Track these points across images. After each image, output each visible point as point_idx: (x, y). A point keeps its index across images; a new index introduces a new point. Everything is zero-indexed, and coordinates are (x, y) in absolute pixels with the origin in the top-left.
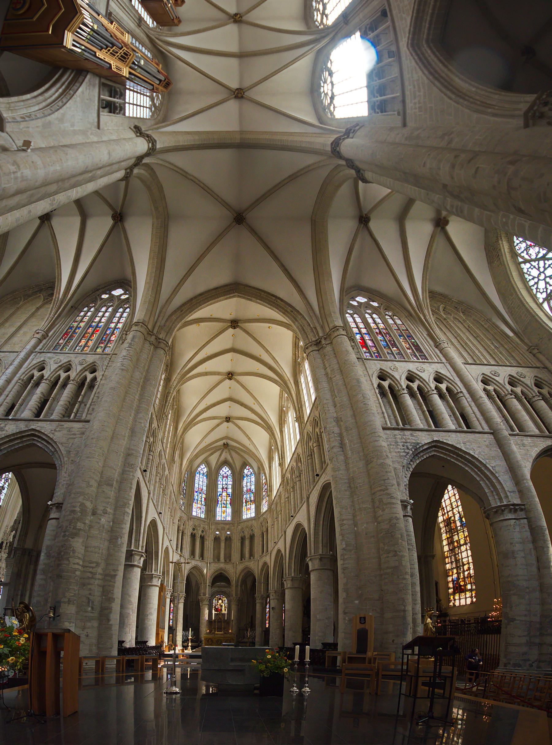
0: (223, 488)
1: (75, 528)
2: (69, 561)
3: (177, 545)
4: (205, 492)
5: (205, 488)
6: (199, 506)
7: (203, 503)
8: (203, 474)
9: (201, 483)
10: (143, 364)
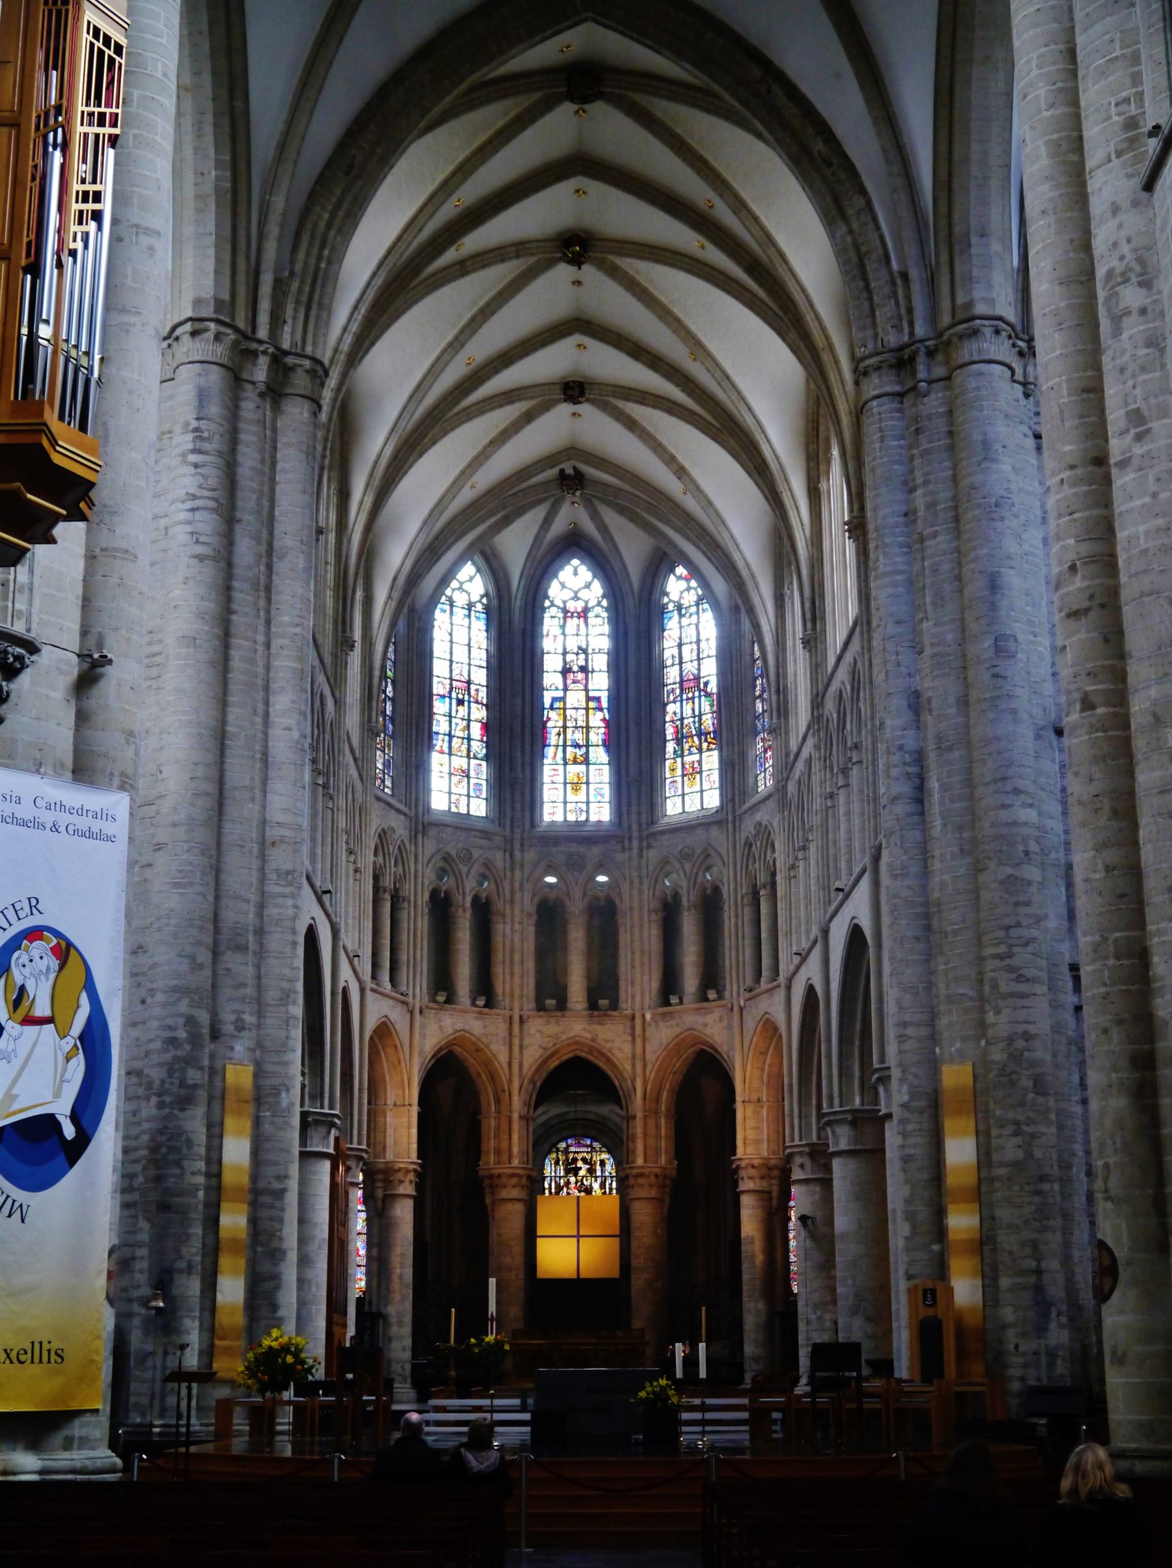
0: (566, 671)
1: (182, 1084)
2: (182, 1168)
3: (375, 954)
4: (483, 695)
5: (480, 677)
6: (460, 762)
7: (478, 748)
8: (470, 606)
9: (460, 654)
10: (254, 496)
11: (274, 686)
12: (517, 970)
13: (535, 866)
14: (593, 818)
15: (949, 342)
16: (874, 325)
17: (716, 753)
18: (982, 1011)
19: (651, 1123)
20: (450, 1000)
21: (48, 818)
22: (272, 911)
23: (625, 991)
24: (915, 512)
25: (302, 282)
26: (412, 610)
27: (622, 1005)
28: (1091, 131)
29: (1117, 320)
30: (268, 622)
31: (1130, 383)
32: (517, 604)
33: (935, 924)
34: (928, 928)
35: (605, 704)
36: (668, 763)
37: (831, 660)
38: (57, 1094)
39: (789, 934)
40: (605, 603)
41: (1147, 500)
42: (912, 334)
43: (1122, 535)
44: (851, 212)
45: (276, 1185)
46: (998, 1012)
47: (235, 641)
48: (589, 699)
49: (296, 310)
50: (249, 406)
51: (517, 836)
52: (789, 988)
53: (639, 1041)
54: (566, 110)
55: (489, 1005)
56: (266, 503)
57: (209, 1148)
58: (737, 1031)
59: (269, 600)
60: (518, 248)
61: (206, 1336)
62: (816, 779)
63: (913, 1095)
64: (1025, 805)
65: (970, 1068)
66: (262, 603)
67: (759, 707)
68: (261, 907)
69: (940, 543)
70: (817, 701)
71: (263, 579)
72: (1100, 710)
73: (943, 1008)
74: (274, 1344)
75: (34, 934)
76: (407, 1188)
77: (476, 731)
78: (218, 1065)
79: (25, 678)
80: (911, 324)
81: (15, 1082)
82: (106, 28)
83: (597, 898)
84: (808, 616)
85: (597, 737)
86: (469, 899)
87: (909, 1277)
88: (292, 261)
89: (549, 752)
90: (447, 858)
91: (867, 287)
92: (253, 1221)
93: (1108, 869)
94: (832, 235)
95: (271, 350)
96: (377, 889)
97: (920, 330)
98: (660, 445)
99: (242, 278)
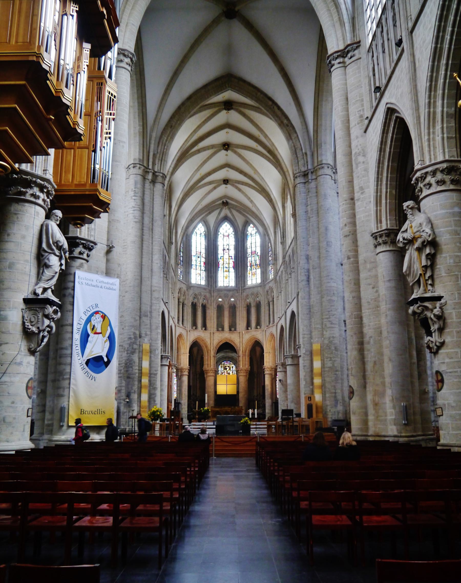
0: (224, 250)
1: (132, 348)
4: (204, 256)
5: (203, 251)
7: (203, 268)
11: (154, 253)
12: (212, 321)
13: (216, 296)
14: (230, 285)
15: (316, 170)
16: (298, 165)
17: (260, 270)
18: (323, 331)
19: (244, 358)
20: (196, 329)
21: (100, 285)
22: (154, 307)
23: (238, 326)
24: (308, 211)
25: (160, 154)
26: (187, 235)
27: (237, 330)
28: (351, 118)
29: (357, 165)
30: (152, 238)
31: (360, 180)
32: (212, 234)
33: (312, 310)
34: (310, 311)
35: (233, 258)
36: (248, 272)
37: (287, 247)
38: (103, 351)
39: (277, 313)
40: (233, 233)
41: (364, 208)
42: (308, 168)
43: (357, 217)
44: (293, 138)
45: (155, 372)
46: (326, 331)
47: (144, 242)
48: (229, 256)
49: (158, 161)
50: (148, 185)
51: (212, 289)
52: (277, 326)
53: (241, 338)
54: (224, 112)
55: (205, 330)
56: (151, 209)
57: (139, 364)
58: (264, 336)
59: (152, 232)
60: (212, 146)
61: (139, 408)
62: (283, 276)
63: (306, 351)
64: (333, 282)
65: (319, 345)
66: (151, 233)
67: (270, 258)
68: (151, 306)
69: (314, 219)
70: (284, 257)
71: (151, 227)
72: (352, 259)
73: (313, 330)
74: (155, 410)
75: (97, 313)
76: (186, 373)
77: (202, 264)
78: (141, 344)
79: (93, 252)
80: (307, 165)
81: (92, 348)
82: (111, 91)
83: (231, 304)
84: (282, 236)
85: (232, 265)
86: (200, 305)
87: (305, 394)
88: (157, 150)
89: (220, 269)
90: (195, 295)
91: (297, 156)
92: (150, 381)
93: (353, 297)
94: (288, 143)
95: (153, 171)
96: (179, 302)
97: (310, 167)
98: (247, 195)
99: (145, 154)
